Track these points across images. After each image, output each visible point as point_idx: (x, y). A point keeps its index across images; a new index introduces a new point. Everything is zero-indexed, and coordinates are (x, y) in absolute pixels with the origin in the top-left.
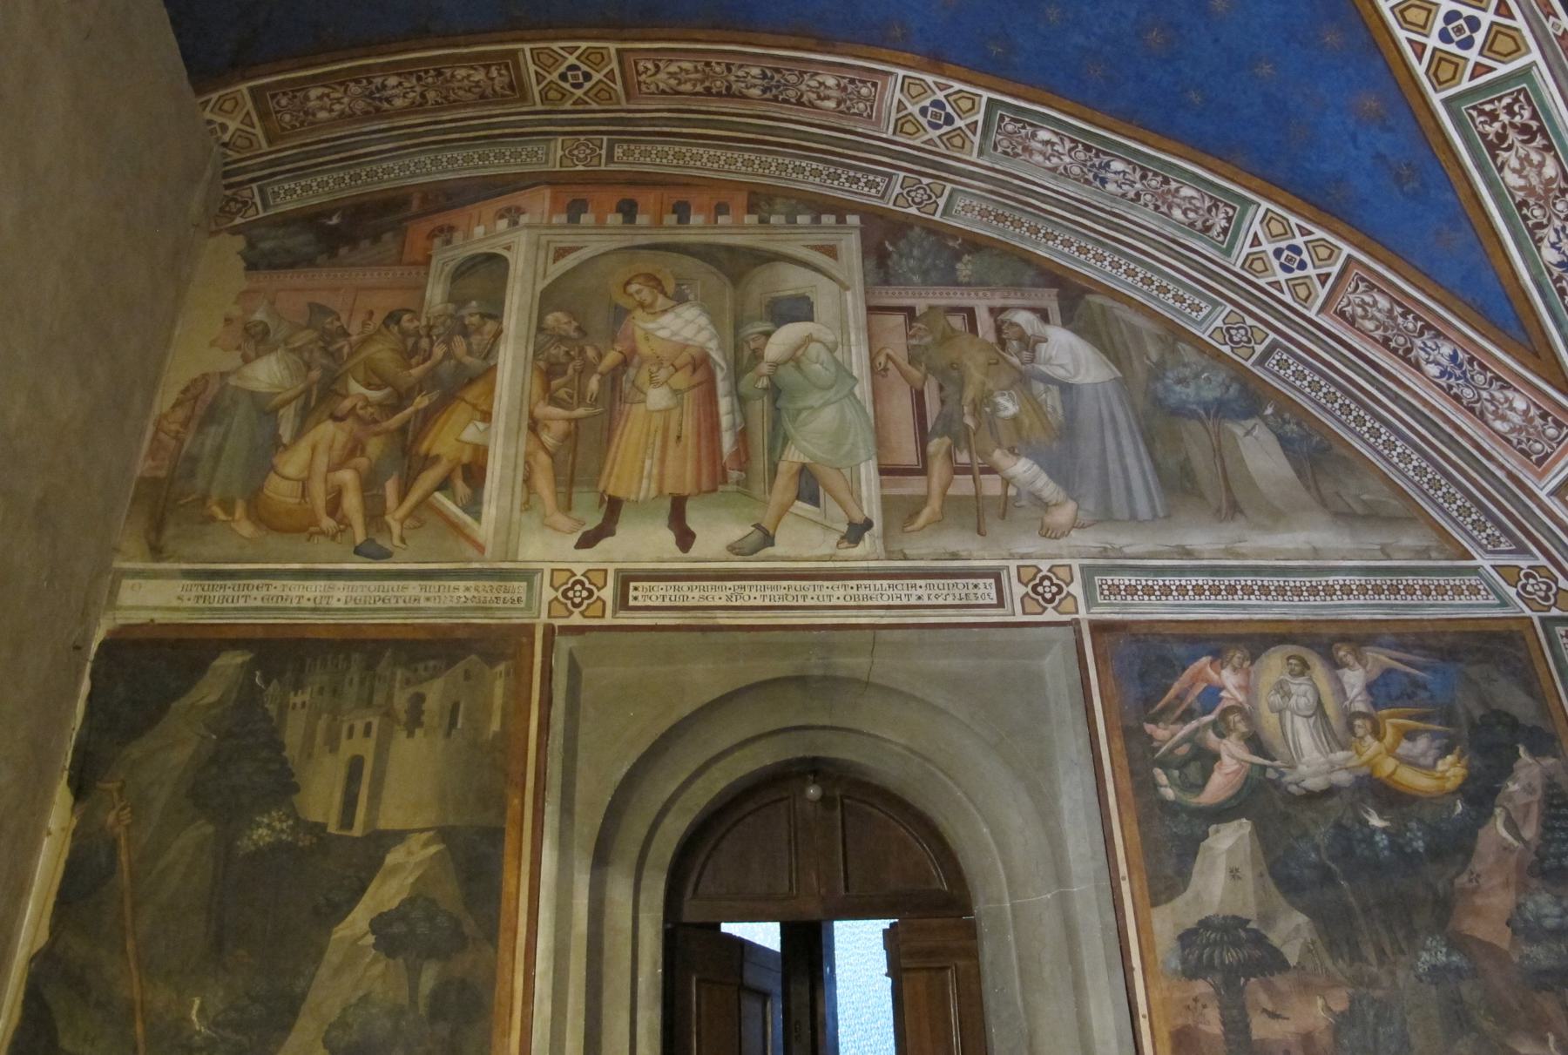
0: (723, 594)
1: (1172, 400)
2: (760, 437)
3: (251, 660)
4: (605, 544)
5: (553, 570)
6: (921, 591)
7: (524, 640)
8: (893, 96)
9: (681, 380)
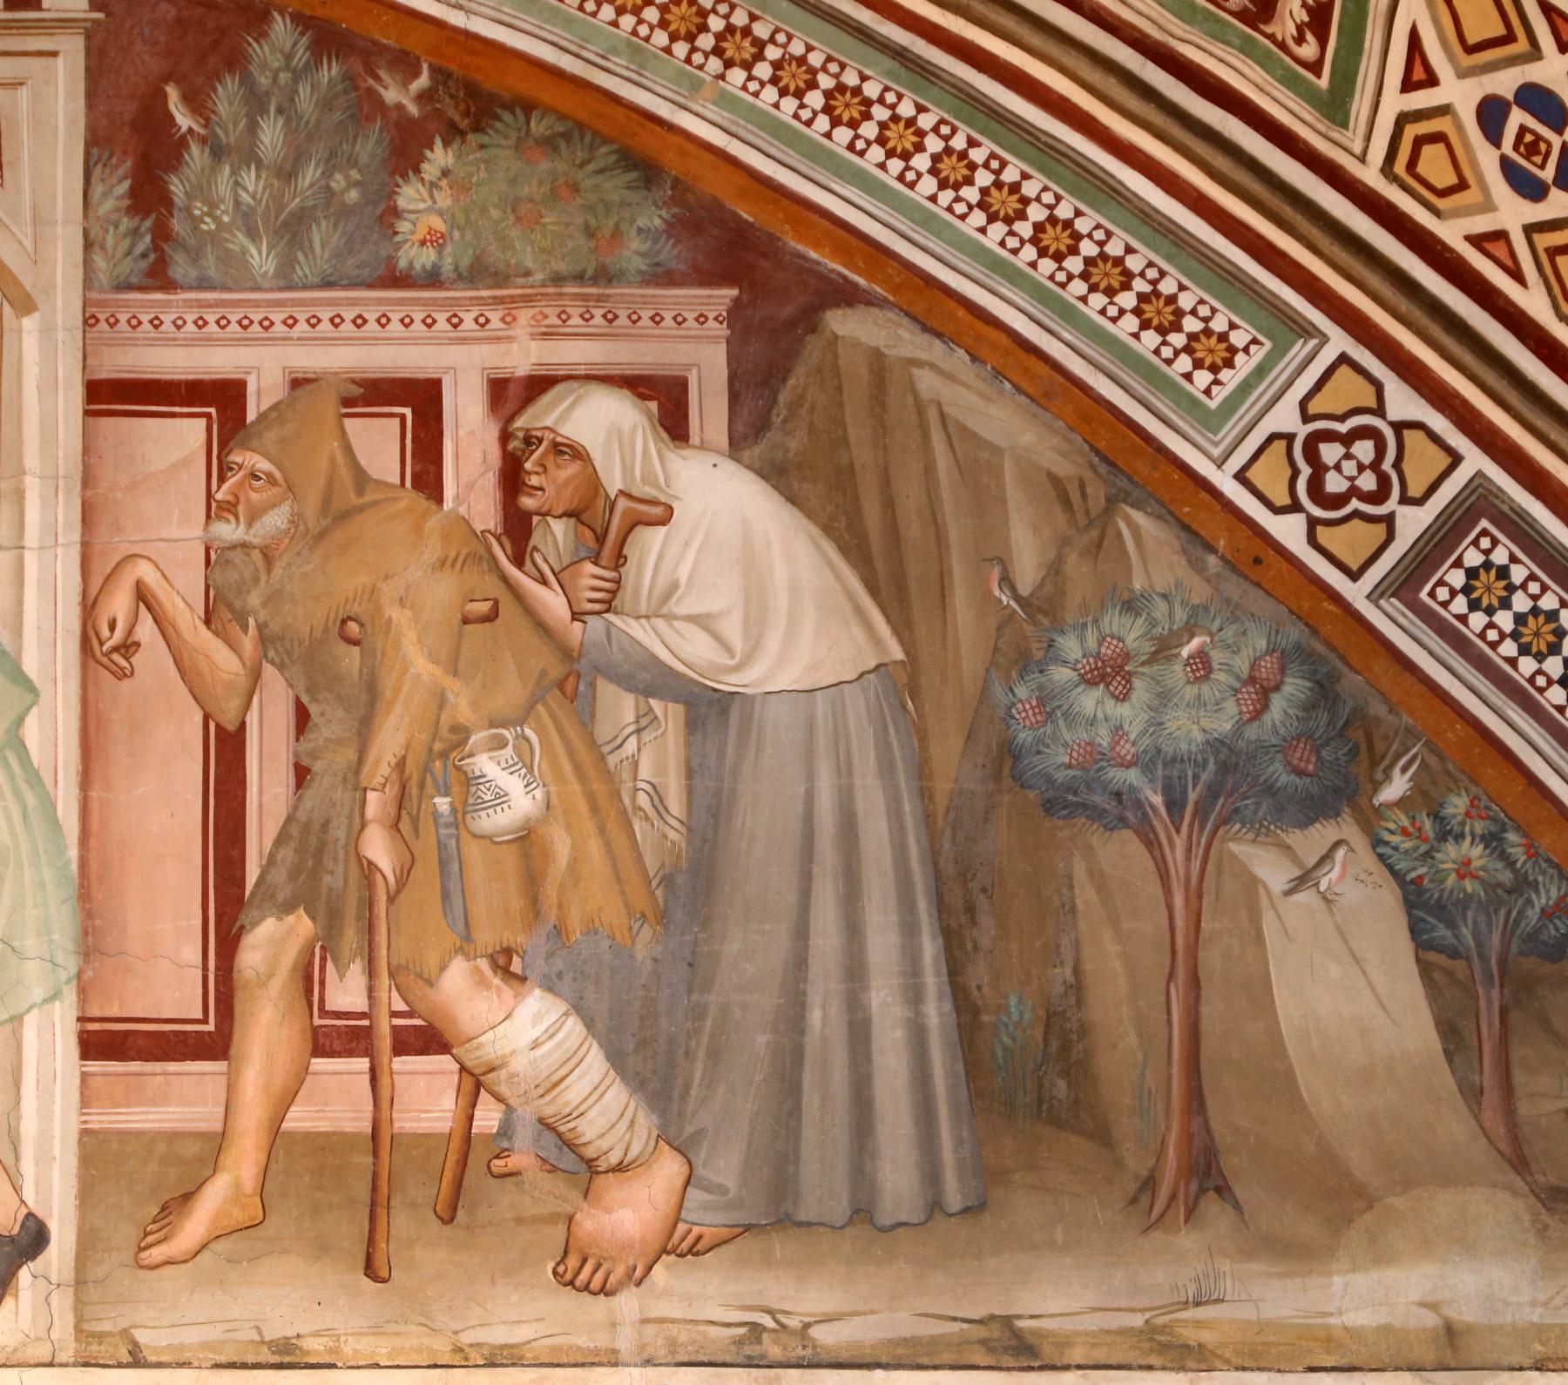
1: (1058, 759)
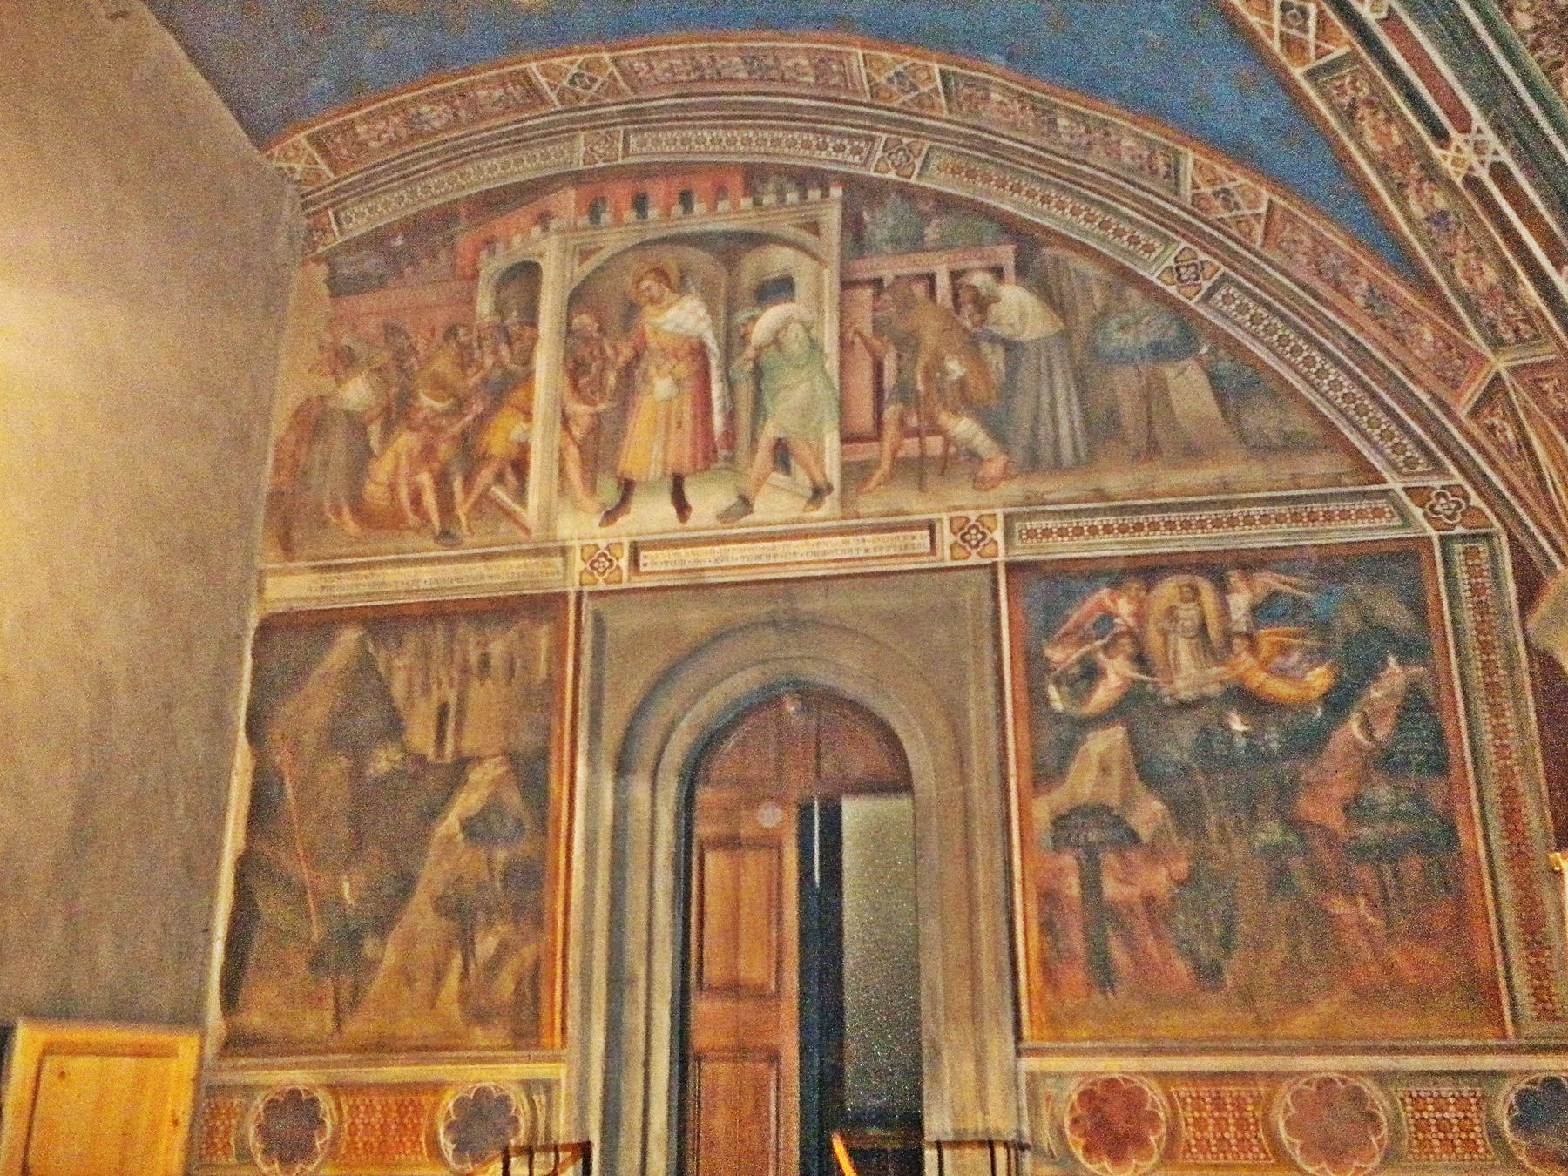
2: (744, 418)
4: (622, 520)
6: (870, 544)
9: (683, 369)
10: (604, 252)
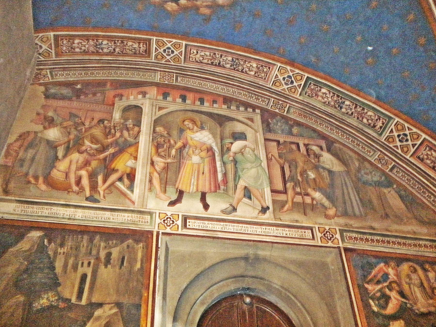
0: (220, 227)
2: (231, 176)
3: (43, 235)
4: (178, 205)
5: (159, 213)
6: (287, 232)
7: (149, 236)
8: (275, 72)
9: (204, 154)
10: (168, 109)
